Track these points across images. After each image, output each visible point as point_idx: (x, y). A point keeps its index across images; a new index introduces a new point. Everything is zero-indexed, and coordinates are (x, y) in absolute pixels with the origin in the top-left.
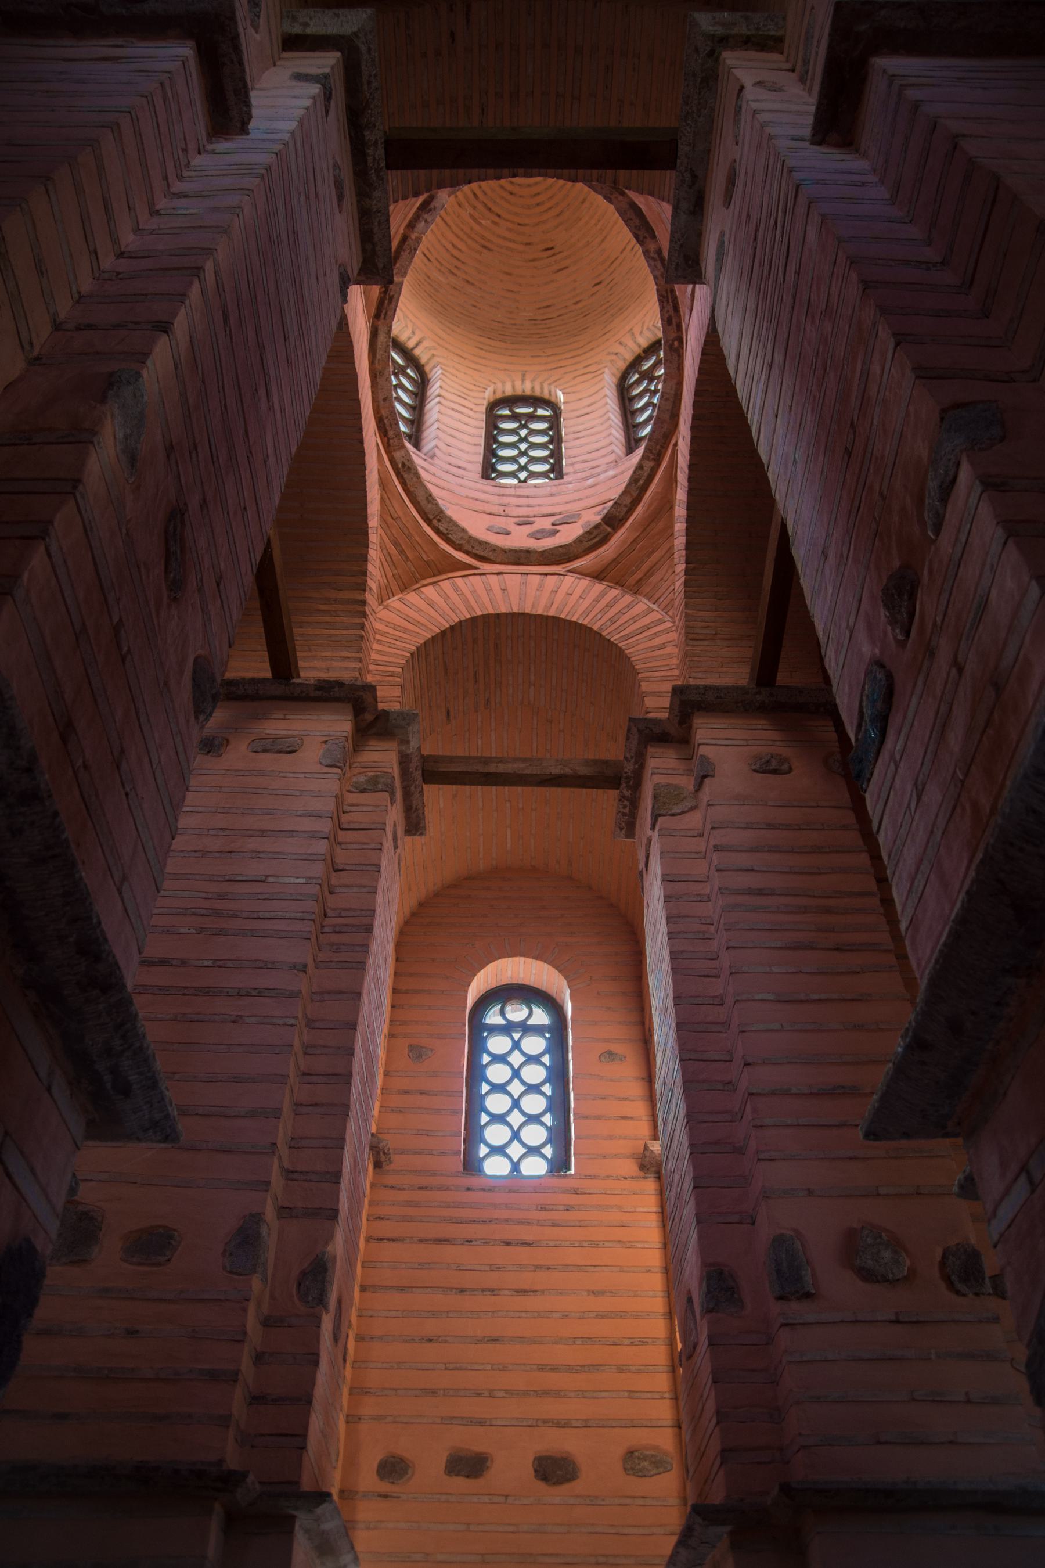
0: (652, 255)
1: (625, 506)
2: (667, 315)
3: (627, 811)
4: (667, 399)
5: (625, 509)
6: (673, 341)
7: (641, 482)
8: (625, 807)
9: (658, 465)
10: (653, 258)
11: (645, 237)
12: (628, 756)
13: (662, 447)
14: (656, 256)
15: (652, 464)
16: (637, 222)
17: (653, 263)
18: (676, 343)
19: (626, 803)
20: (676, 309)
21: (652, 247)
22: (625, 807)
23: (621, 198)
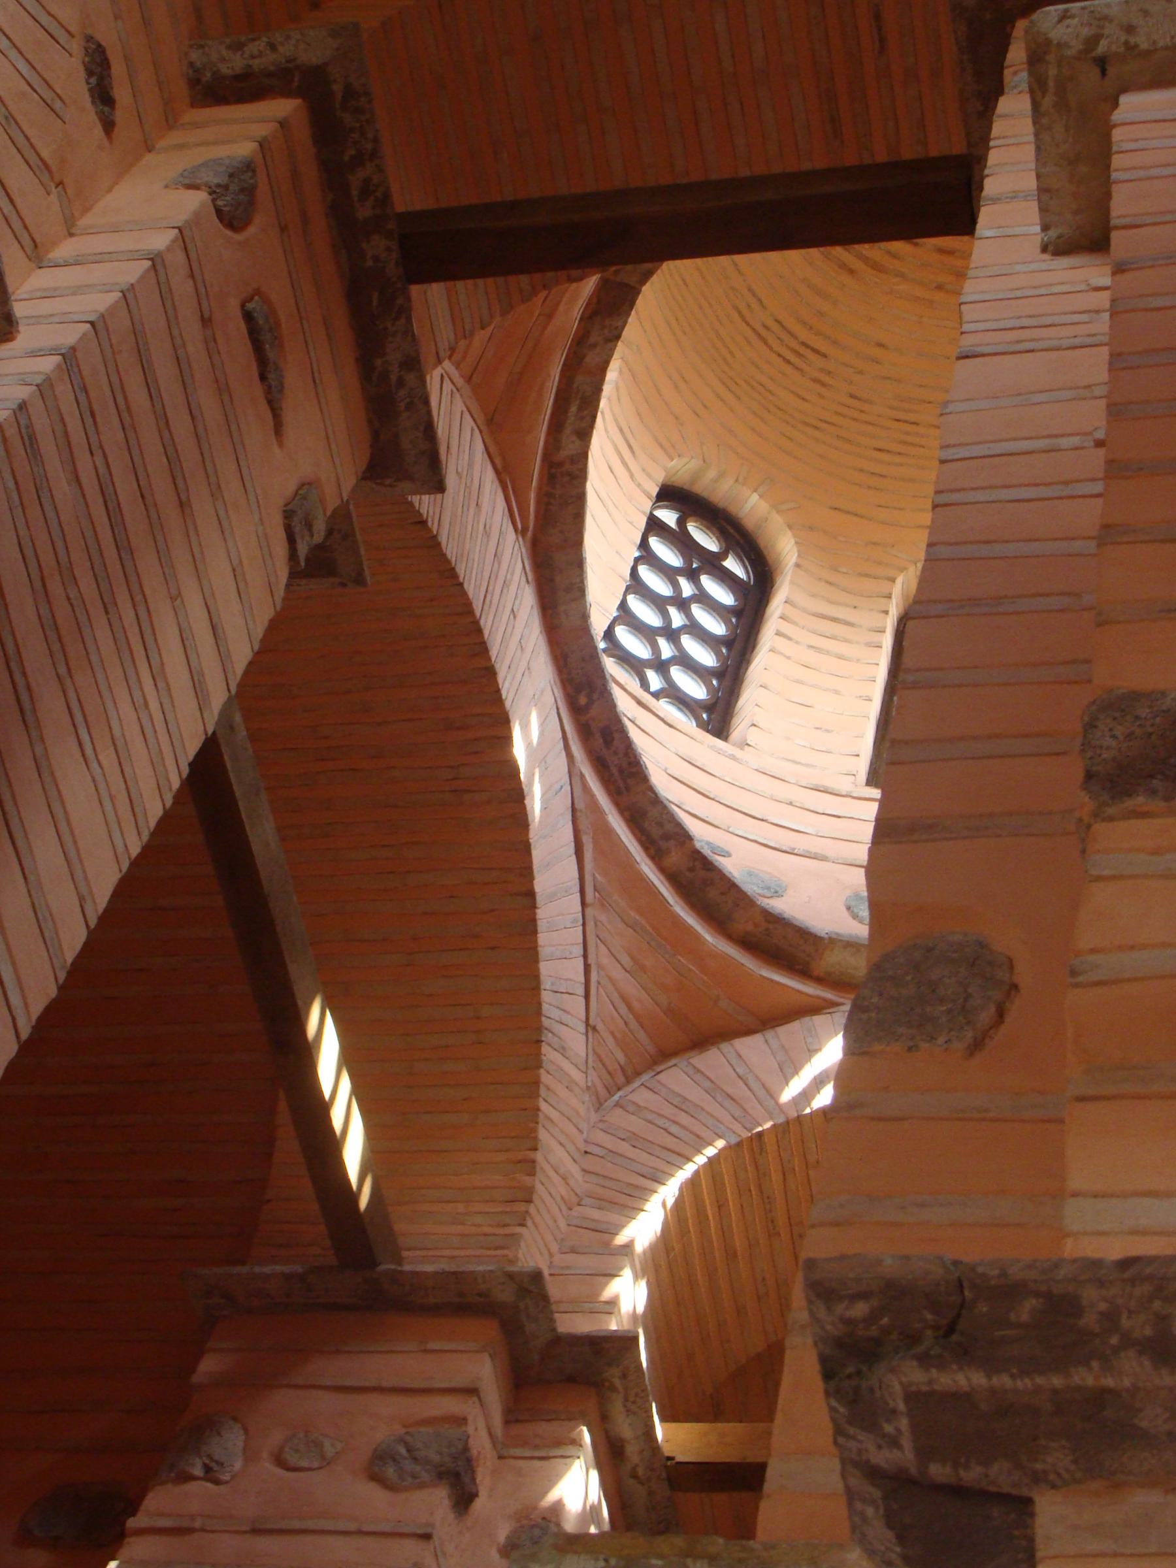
0: (672, 843)
1: (594, 346)
2: (616, 743)
3: (356, 179)
4: (568, 590)
5: (592, 340)
6: (591, 702)
7: (573, 409)
8: (366, 190)
9: (546, 456)
10: (666, 837)
11: (691, 870)
12: (410, 378)
13: (549, 495)
14: (664, 845)
15: (563, 454)
16: (713, 894)
17: (669, 827)
18: (583, 701)
19: (364, 212)
20: (600, 765)
21: (675, 858)
22: (366, 190)
23: (750, 927)
